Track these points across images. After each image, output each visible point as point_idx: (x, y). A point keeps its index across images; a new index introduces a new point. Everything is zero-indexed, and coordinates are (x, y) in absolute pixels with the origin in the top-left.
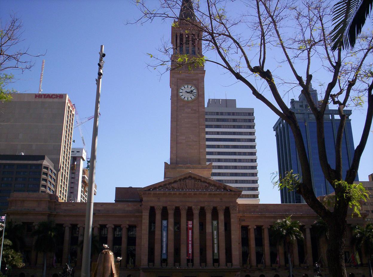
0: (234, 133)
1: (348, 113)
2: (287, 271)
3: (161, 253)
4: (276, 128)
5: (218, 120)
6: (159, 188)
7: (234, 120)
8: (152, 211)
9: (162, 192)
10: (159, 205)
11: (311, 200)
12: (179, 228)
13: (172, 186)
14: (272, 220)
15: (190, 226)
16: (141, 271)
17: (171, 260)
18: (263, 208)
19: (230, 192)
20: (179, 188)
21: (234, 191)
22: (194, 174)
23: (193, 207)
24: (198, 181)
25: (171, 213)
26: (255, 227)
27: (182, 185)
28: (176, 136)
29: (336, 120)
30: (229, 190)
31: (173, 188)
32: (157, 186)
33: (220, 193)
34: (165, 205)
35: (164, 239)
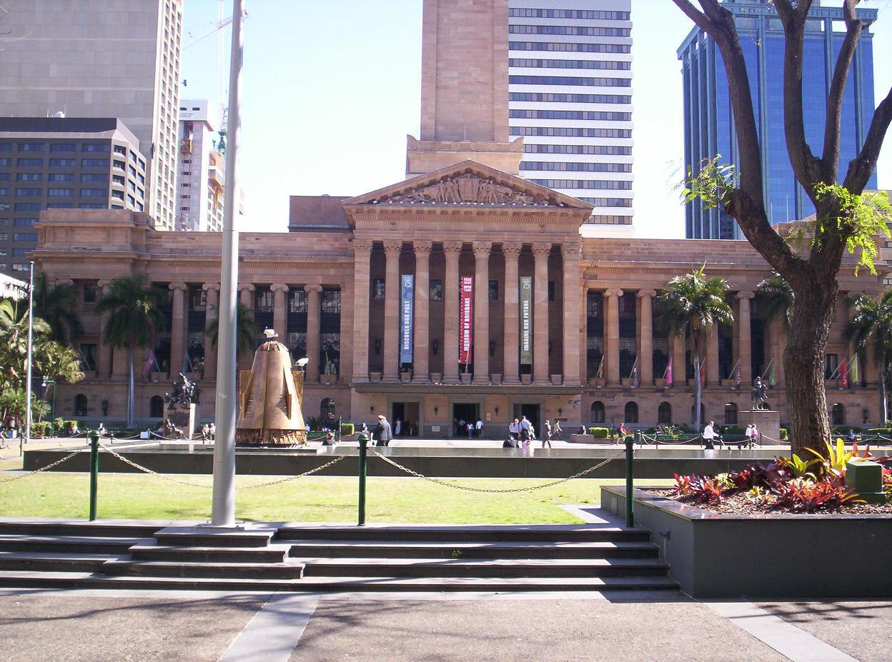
0: (580, 64)
1: (868, 17)
2: (690, 394)
3: (400, 351)
4: (684, 53)
5: (541, 30)
6: (395, 198)
7: (581, 31)
8: (378, 252)
9: (402, 209)
10: (393, 237)
11: (756, 231)
12: (441, 294)
13: (424, 193)
14: (662, 277)
15: (468, 289)
16: (353, 390)
17: (422, 365)
18: (642, 249)
19: (565, 211)
20: (441, 198)
21: (574, 207)
22: (479, 165)
23: (475, 244)
24: (487, 181)
25: (422, 258)
26: (621, 293)
27: (449, 190)
28: (437, 69)
29: (836, 36)
30: (562, 205)
32: (390, 194)
33: (540, 211)
34: (408, 239)
35: (407, 319)
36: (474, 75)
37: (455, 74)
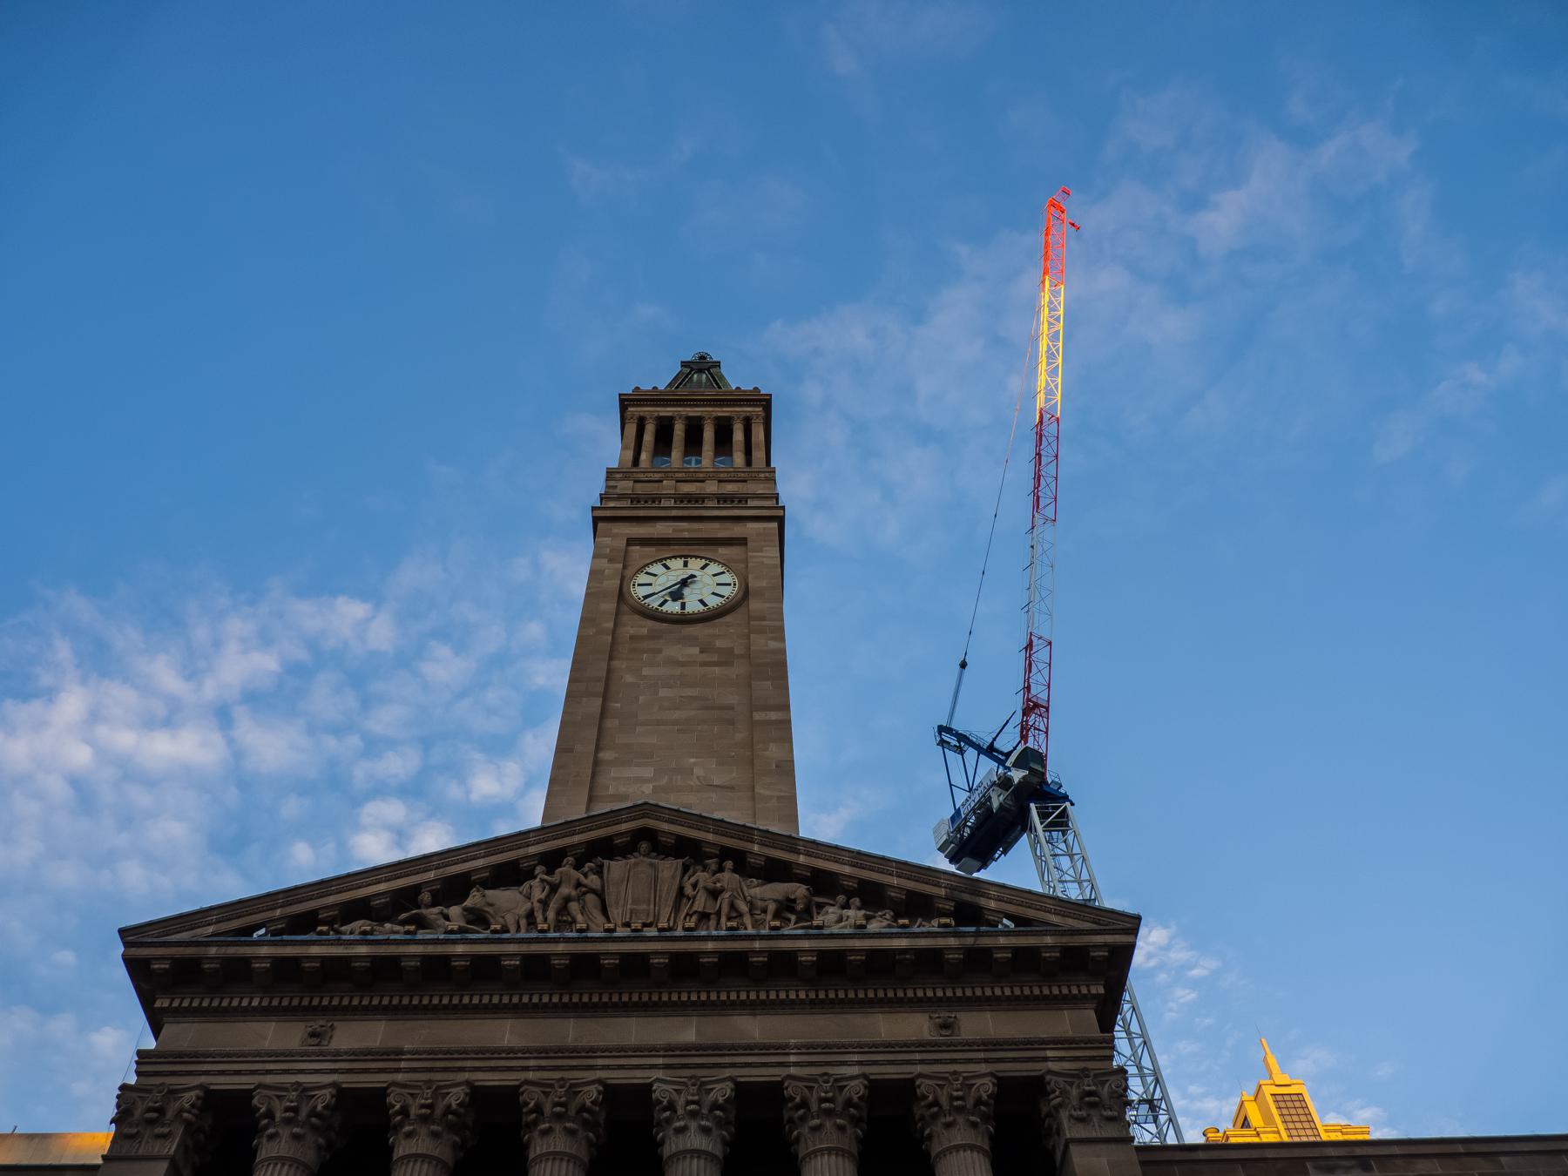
22: (678, 816)
23: (661, 1092)
27: (565, 890)
31: (478, 918)
36: (698, 771)
37: (648, 772)
